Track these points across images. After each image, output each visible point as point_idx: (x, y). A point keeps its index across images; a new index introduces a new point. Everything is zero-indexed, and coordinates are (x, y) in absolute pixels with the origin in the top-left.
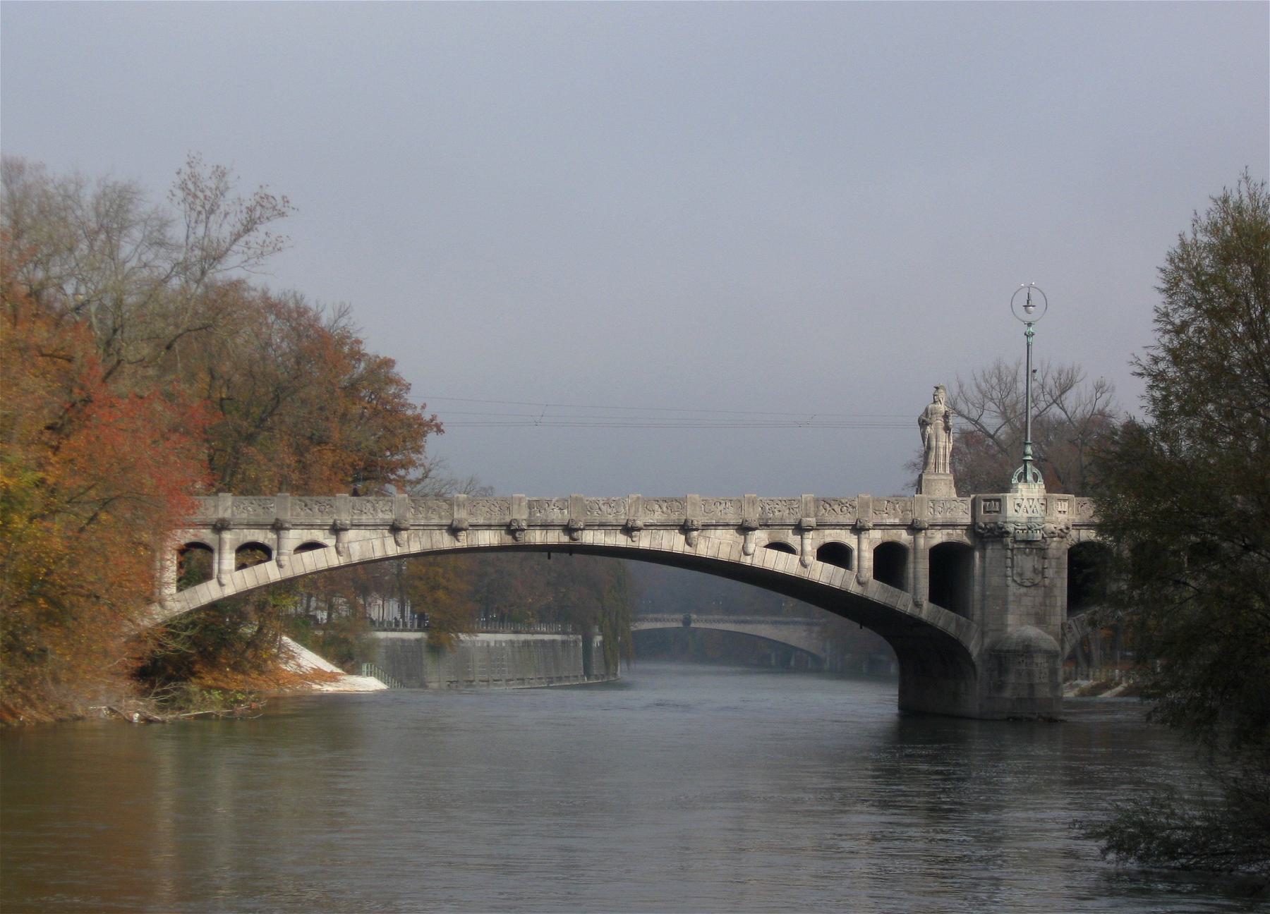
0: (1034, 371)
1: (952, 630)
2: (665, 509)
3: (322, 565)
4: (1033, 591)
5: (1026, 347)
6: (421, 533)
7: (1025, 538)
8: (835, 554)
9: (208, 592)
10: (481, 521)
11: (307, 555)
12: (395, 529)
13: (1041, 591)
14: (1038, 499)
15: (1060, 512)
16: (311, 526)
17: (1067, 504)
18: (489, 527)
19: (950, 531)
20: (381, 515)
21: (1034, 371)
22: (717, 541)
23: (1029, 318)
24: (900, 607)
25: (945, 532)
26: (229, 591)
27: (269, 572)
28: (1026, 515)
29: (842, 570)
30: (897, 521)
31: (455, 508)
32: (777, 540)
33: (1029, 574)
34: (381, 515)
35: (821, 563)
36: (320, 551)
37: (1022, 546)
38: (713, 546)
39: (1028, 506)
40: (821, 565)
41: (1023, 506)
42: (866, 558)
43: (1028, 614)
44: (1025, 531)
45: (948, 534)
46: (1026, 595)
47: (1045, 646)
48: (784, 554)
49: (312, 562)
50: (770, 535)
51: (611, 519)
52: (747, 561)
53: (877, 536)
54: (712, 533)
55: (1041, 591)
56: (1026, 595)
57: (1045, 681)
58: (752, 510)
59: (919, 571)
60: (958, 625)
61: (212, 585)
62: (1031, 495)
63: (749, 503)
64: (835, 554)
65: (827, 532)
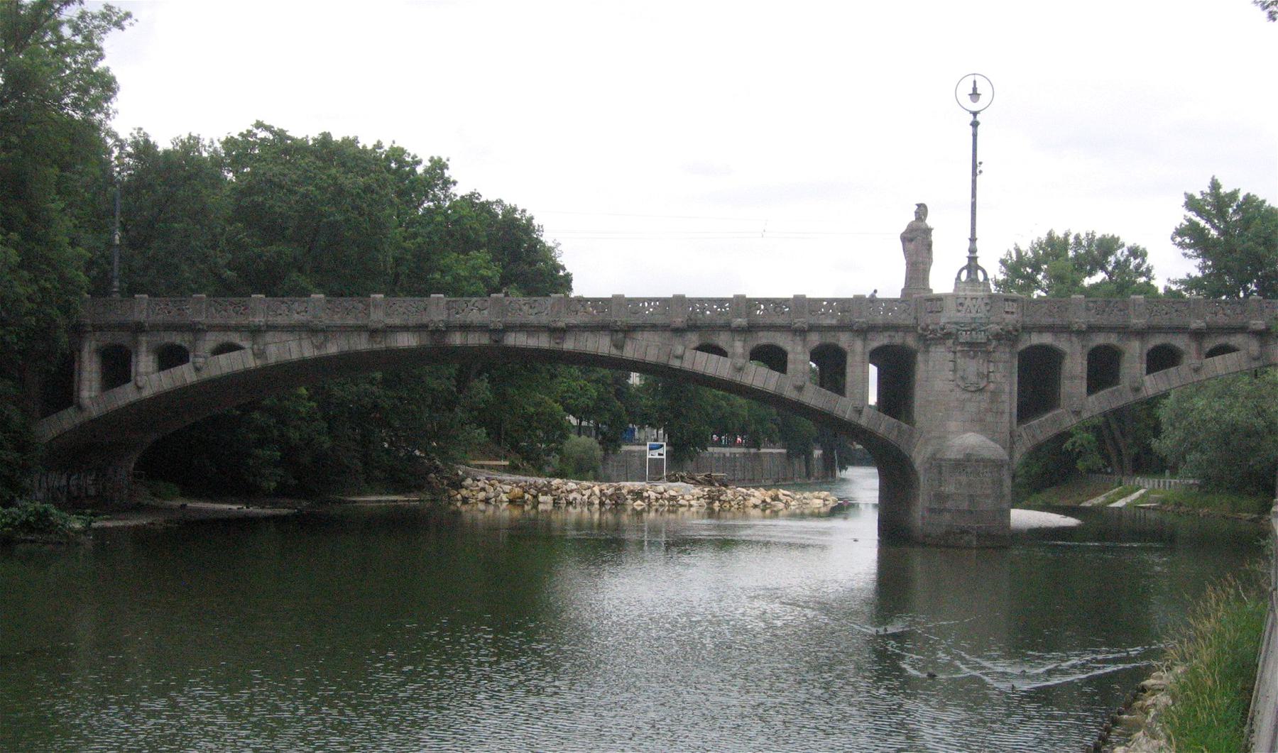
0: (980, 163)
1: (892, 437)
3: (238, 367)
4: (978, 397)
5: (971, 138)
7: (969, 340)
9: (126, 395)
10: (397, 321)
11: (222, 358)
13: (986, 396)
15: (1007, 312)
16: (226, 328)
17: (1015, 305)
18: (405, 328)
19: (893, 334)
21: (980, 163)
22: (644, 343)
23: (975, 107)
24: (838, 412)
25: (886, 334)
26: (147, 393)
27: (185, 374)
29: (777, 374)
31: (372, 309)
33: (973, 378)
36: (235, 354)
37: (965, 349)
40: (777, 376)
41: (965, 307)
43: (973, 420)
46: (970, 400)
47: (986, 454)
48: (715, 357)
49: (227, 364)
51: (532, 319)
52: (676, 364)
53: (815, 339)
54: (639, 335)
55: (986, 396)
56: (970, 400)
61: (129, 387)
65: (761, 334)
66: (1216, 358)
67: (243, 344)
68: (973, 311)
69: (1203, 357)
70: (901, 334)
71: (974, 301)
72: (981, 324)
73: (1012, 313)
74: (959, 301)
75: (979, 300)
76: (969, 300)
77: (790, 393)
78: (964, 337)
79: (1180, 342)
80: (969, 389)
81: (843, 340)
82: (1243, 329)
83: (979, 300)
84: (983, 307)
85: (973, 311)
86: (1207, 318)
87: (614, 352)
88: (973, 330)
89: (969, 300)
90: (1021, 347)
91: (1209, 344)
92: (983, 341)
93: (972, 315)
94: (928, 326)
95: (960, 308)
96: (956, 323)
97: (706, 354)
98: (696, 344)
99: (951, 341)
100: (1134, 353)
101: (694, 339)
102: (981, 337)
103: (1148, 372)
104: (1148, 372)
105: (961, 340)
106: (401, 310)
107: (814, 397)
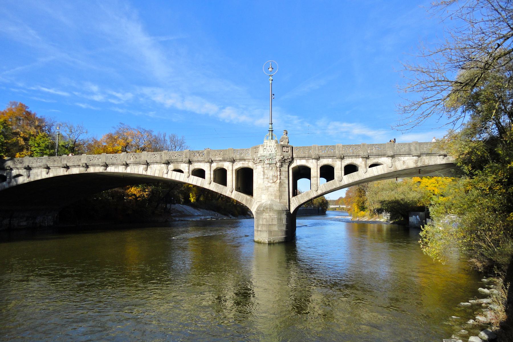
1: (244, 202)
2: (134, 158)
6: (53, 169)
7: (268, 163)
8: (200, 173)
12: (48, 168)
19: (243, 162)
20: (39, 164)
22: (154, 169)
25: (241, 162)
28: (268, 153)
29: (201, 179)
30: (221, 159)
31: (63, 160)
32: (176, 168)
33: (271, 178)
34: (39, 164)
35: (193, 176)
38: (153, 171)
42: (209, 174)
44: (268, 160)
45: (243, 163)
46: (270, 186)
48: (179, 173)
50: (174, 166)
53: (215, 166)
57: (276, 223)
58: (165, 156)
59: (231, 178)
60: (247, 200)
63: (165, 154)
64: (200, 173)
66: (373, 168)
67: (21, 173)
69: (368, 167)
70: (247, 162)
71: (270, 147)
73: (287, 152)
76: (268, 146)
77: (206, 186)
78: (267, 162)
79: (358, 162)
80: (270, 182)
81: (227, 165)
82: (384, 155)
83: (272, 147)
84: (274, 149)
86: (369, 152)
87: (144, 173)
89: (268, 146)
90: (293, 165)
91: (370, 162)
93: (270, 153)
95: (265, 150)
96: (264, 156)
97: (176, 172)
98: (173, 169)
99: (262, 164)
100: (339, 167)
101: (171, 167)
102: (274, 162)
103: (345, 174)
104: (345, 174)
105: (266, 163)
106: (72, 160)
107: (214, 187)
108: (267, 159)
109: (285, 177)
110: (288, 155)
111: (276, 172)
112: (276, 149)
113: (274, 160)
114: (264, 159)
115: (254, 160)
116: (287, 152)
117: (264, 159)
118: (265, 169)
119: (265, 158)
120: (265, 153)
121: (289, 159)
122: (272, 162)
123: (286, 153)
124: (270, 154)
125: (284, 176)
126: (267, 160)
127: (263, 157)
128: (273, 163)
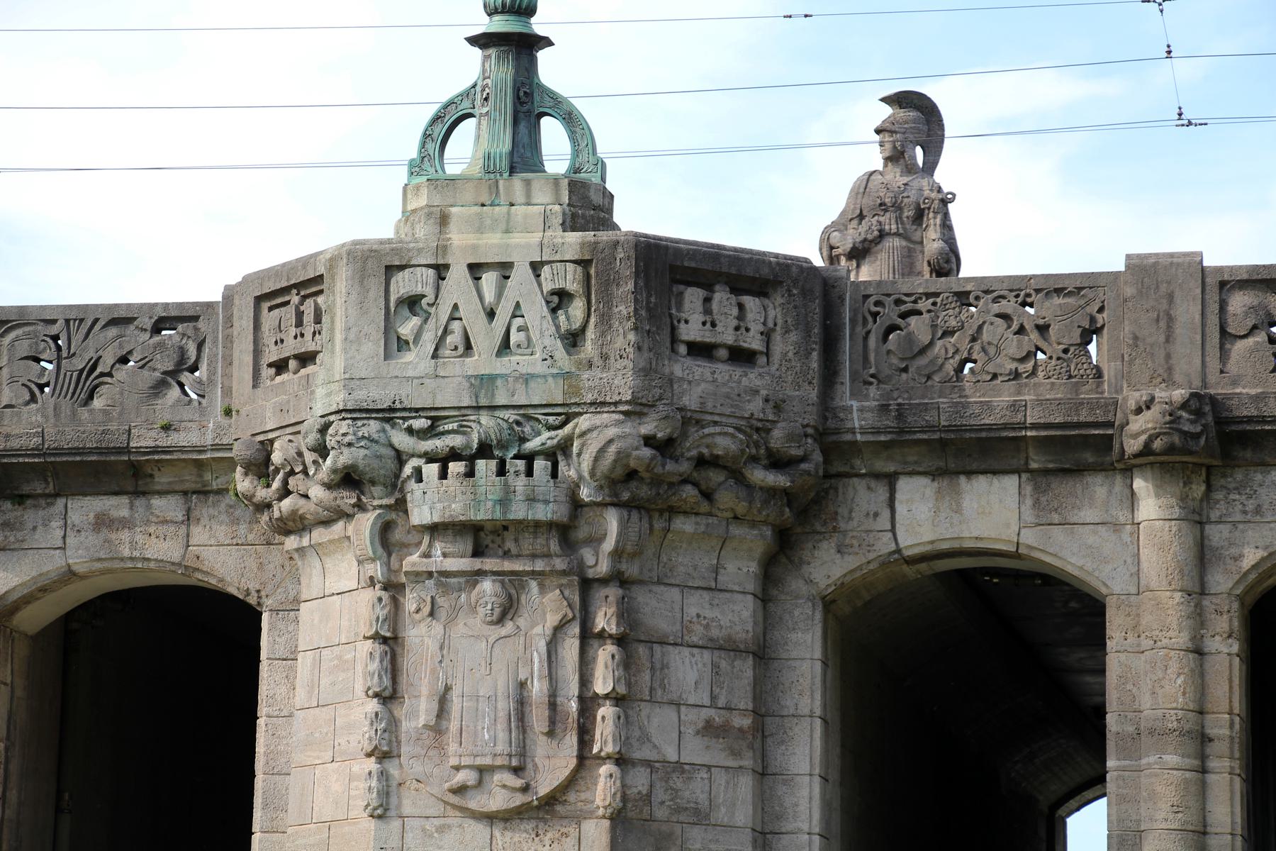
14: (536, 267)
15: (701, 350)
19: (118, 506)
25: (83, 509)
39: (472, 317)
44: (456, 467)
62: (491, 245)
68: (485, 337)
71: (489, 280)
72: (526, 413)
73: (741, 356)
74: (403, 285)
75: (521, 273)
76: (458, 274)
83: (521, 273)
84: (536, 312)
85: (485, 337)
88: (484, 450)
89: (458, 274)
92: (542, 513)
93: (483, 361)
94: (267, 447)
96: (389, 415)
105: (421, 514)
108: (444, 460)
109: (709, 729)
110: (755, 407)
111: (570, 648)
112: (577, 309)
113: (540, 465)
114: (400, 458)
115: (261, 467)
116: (741, 356)
117: (400, 458)
118: (410, 602)
119: (401, 440)
120: (416, 360)
121: (777, 462)
122: (504, 502)
123: (724, 371)
124: (487, 381)
125: (694, 718)
126: (432, 470)
127: (373, 427)
128: (519, 511)
